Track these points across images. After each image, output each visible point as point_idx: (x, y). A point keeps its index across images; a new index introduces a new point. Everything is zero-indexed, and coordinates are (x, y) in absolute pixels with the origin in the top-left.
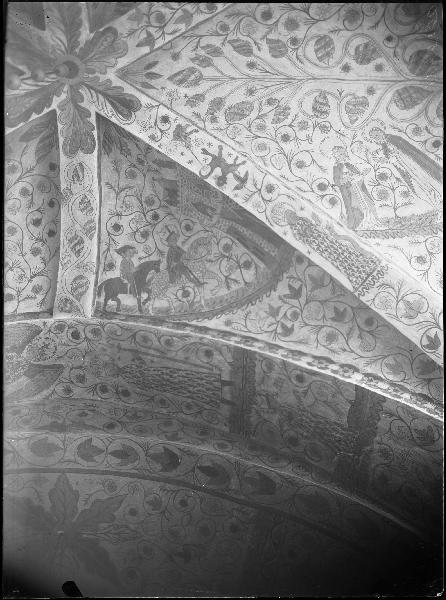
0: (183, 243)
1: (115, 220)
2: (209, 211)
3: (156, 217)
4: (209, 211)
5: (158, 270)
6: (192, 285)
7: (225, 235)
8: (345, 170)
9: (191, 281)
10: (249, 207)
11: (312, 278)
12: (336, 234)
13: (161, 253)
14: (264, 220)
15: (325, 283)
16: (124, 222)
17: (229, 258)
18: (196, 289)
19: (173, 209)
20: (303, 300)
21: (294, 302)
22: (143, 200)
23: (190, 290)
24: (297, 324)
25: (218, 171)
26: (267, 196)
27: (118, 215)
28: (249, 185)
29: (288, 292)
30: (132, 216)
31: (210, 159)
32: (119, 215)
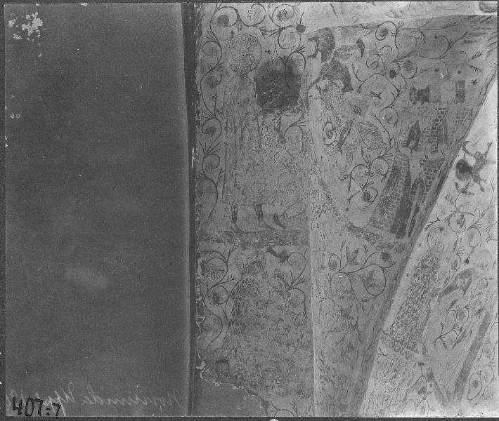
0: (371, 114)
1: (392, 28)
2: (412, 143)
3: (393, 74)
4: (412, 143)
5: (344, 90)
6: (338, 139)
7: (391, 165)
8: (467, 280)
9: (341, 138)
10: (441, 201)
11: (371, 274)
12: (430, 300)
13: (359, 91)
14: (430, 220)
15: (370, 289)
16: (390, 40)
17: (369, 174)
18: (335, 143)
19: (405, 95)
20: (347, 269)
21: (345, 260)
22: (411, 58)
23: (334, 137)
24: (328, 270)
25: (472, 162)
26: (453, 221)
27: (397, 32)
28: (462, 199)
29: (352, 249)
30: (394, 48)
31: (483, 152)
32: (396, 34)
